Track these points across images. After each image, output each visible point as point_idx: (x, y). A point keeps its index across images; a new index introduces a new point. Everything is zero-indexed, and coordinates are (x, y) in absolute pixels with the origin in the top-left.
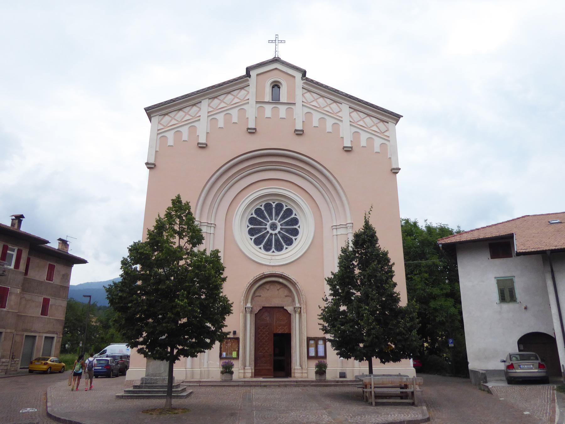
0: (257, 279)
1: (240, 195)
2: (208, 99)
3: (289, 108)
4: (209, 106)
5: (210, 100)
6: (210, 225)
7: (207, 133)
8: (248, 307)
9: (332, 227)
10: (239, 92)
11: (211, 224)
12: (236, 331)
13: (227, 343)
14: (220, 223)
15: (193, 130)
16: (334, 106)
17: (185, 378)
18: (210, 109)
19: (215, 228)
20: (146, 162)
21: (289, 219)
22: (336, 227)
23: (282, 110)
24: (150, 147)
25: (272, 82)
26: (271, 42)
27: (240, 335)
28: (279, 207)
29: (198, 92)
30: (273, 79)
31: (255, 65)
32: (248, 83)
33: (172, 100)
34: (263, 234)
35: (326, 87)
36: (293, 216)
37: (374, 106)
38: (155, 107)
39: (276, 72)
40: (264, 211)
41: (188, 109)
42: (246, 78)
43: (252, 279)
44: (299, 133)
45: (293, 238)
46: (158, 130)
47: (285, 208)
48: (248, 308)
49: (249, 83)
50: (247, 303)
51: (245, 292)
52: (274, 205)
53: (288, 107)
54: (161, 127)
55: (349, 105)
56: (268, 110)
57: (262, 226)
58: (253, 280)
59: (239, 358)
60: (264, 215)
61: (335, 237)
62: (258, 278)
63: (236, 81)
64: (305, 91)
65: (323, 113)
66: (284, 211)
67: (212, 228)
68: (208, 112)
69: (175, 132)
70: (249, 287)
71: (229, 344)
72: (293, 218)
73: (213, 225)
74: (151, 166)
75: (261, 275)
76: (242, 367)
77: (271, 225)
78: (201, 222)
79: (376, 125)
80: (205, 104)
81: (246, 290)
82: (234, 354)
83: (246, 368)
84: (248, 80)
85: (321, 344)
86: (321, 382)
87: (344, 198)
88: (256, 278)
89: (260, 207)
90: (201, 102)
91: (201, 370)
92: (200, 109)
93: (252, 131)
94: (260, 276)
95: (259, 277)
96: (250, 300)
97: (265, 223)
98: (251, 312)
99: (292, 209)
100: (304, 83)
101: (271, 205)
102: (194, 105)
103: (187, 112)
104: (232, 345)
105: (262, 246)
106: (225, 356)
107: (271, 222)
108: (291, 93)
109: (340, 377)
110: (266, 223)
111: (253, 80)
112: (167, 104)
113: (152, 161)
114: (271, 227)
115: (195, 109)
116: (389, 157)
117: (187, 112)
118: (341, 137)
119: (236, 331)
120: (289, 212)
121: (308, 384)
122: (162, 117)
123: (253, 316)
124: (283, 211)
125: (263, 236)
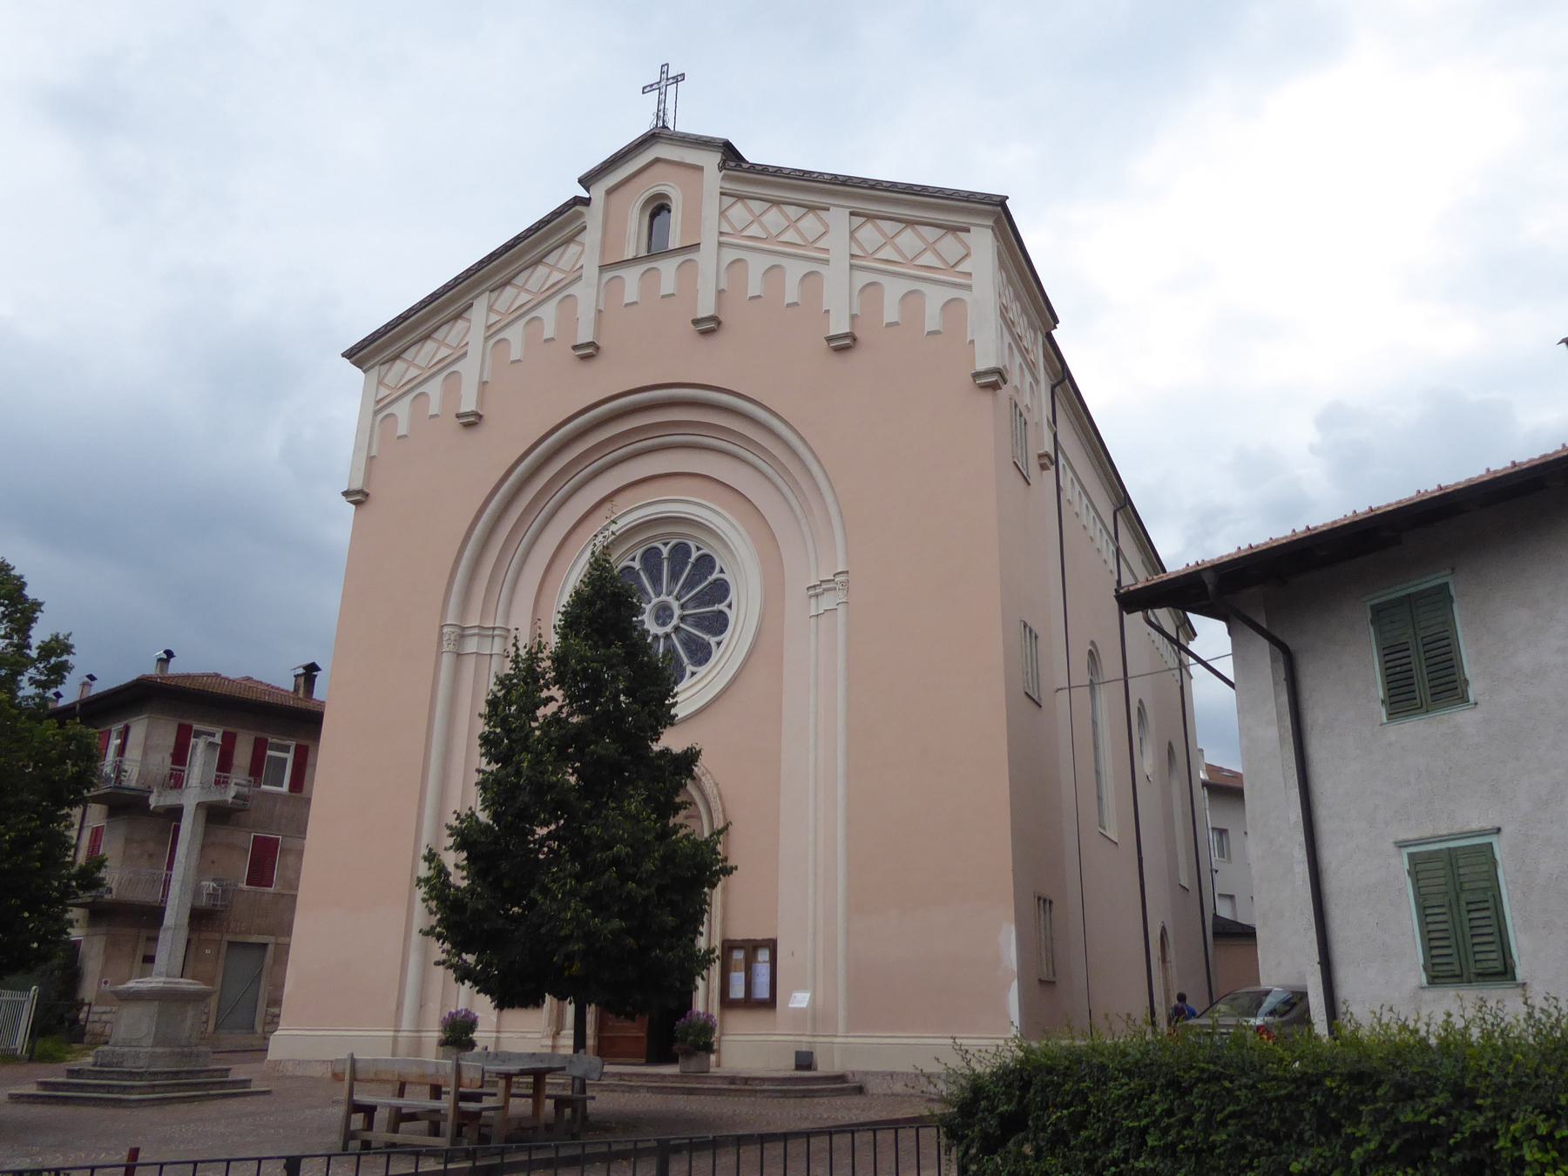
2: (488, 292)
9: (808, 589)
11: (494, 629)
20: (346, 489)
22: (816, 591)
23: (668, 269)
25: (646, 202)
26: (649, 89)
28: (681, 551)
29: (457, 281)
32: (583, 220)
33: (399, 316)
35: (776, 172)
37: (915, 188)
38: (366, 343)
39: (658, 168)
40: (642, 573)
42: (574, 209)
44: (709, 327)
45: (713, 640)
47: (695, 555)
49: (583, 222)
52: (665, 551)
53: (680, 262)
54: (384, 392)
55: (849, 207)
66: (694, 565)
68: (489, 327)
73: (496, 632)
76: (551, 1030)
78: (464, 629)
79: (931, 247)
83: (563, 1032)
84: (581, 214)
85: (764, 962)
86: (685, 1080)
87: (829, 499)
90: (472, 305)
93: (589, 352)
101: (657, 551)
108: (693, 219)
109: (798, 1067)
113: (357, 485)
114: (657, 618)
118: (825, 311)
120: (706, 562)
121: (639, 1084)
122: (386, 366)
124: (689, 567)
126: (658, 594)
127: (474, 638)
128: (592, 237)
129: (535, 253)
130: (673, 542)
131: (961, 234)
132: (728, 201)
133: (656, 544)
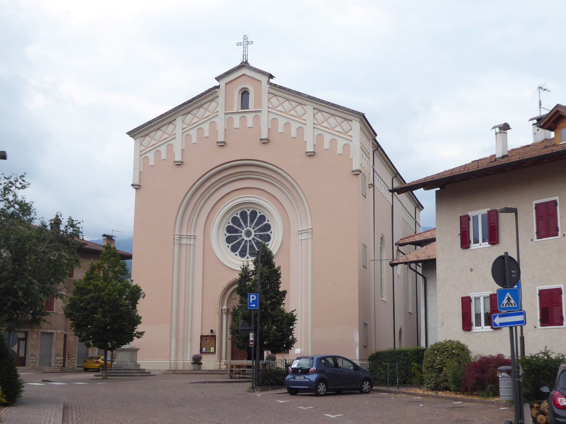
0: (232, 284)
1: (217, 206)
3: (256, 115)
4: (183, 122)
5: (184, 116)
6: (190, 237)
7: (183, 150)
8: (223, 309)
10: (210, 105)
11: (191, 236)
12: (213, 330)
13: (206, 340)
14: (199, 234)
15: (170, 148)
16: (299, 108)
17: (169, 369)
18: (185, 126)
19: (195, 239)
21: (263, 226)
22: (301, 232)
23: (250, 117)
24: (134, 169)
27: (217, 334)
28: (254, 213)
30: (238, 89)
31: (222, 74)
32: (217, 94)
34: (239, 241)
36: (266, 222)
38: (136, 130)
39: (244, 77)
40: (240, 219)
41: (165, 127)
43: (226, 284)
44: (265, 142)
46: (141, 152)
48: (224, 309)
49: (218, 95)
50: (224, 305)
51: (220, 296)
52: (248, 213)
53: (256, 115)
54: (143, 148)
56: (237, 119)
57: (238, 233)
58: (227, 285)
59: (215, 353)
60: (240, 223)
61: (300, 241)
62: (231, 282)
63: (205, 94)
64: (272, 96)
65: (288, 118)
66: (258, 218)
67: (192, 240)
68: (183, 129)
69: (155, 152)
70: (224, 292)
71: (208, 341)
72: (266, 224)
73: (192, 237)
74: (137, 187)
75: (234, 280)
77: (246, 232)
78: (181, 235)
79: (339, 124)
80: (179, 120)
81: (221, 294)
82: (212, 350)
83: (222, 361)
84: (216, 92)
87: (306, 205)
88: (229, 283)
89: (236, 216)
90: (176, 119)
91: (183, 362)
92: (175, 125)
93: (222, 145)
94: (233, 281)
95: (232, 282)
96: (225, 303)
97: (241, 231)
98: (227, 313)
99: (265, 215)
100: (269, 87)
101: (246, 213)
102: (170, 123)
103: (164, 131)
104: (210, 341)
105: (237, 253)
106: (205, 351)
107: (245, 229)
110: (241, 230)
111: (221, 93)
112: (145, 126)
113: (137, 182)
115: (171, 126)
116: (351, 158)
117: (164, 131)
118: (305, 142)
119: (213, 330)
120: (263, 218)
123: (230, 316)
124: (257, 218)
125: (239, 243)
126: (247, 227)
127: (184, 239)
128: (221, 100)
129: (200, 103)
130: (251, 210)
131: (349, 122)
132: (271, 96)
133: (246, 210)
